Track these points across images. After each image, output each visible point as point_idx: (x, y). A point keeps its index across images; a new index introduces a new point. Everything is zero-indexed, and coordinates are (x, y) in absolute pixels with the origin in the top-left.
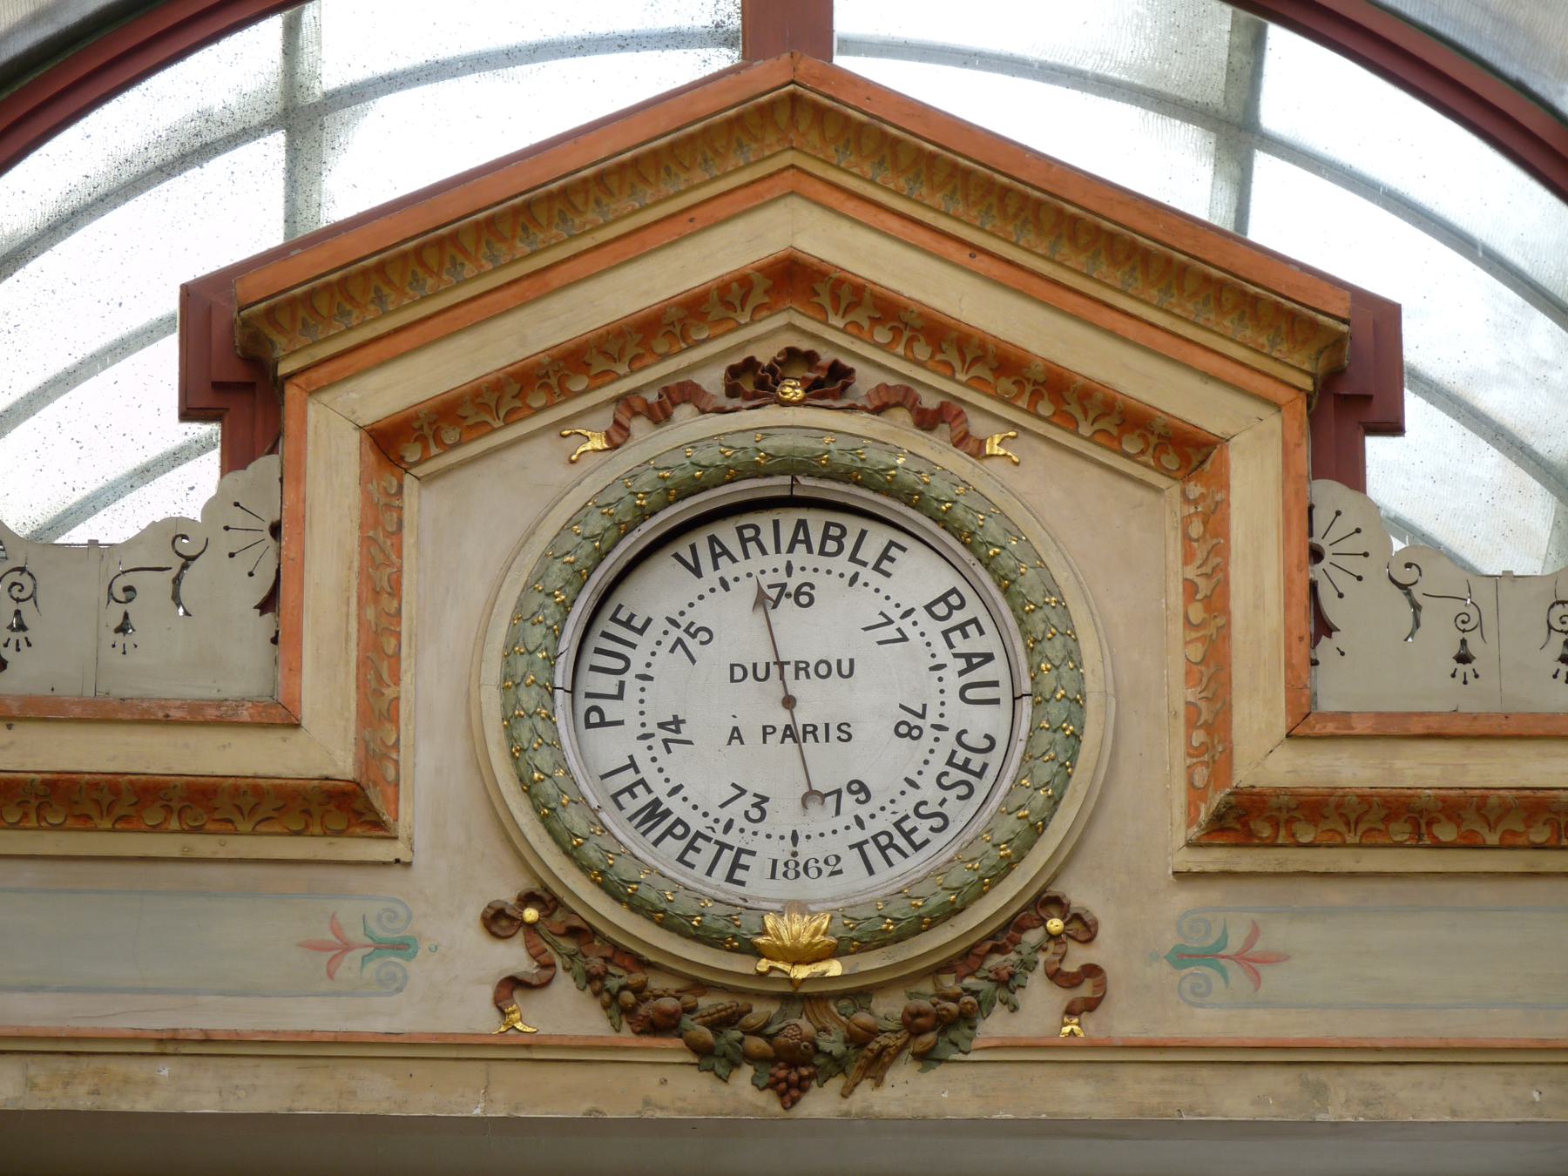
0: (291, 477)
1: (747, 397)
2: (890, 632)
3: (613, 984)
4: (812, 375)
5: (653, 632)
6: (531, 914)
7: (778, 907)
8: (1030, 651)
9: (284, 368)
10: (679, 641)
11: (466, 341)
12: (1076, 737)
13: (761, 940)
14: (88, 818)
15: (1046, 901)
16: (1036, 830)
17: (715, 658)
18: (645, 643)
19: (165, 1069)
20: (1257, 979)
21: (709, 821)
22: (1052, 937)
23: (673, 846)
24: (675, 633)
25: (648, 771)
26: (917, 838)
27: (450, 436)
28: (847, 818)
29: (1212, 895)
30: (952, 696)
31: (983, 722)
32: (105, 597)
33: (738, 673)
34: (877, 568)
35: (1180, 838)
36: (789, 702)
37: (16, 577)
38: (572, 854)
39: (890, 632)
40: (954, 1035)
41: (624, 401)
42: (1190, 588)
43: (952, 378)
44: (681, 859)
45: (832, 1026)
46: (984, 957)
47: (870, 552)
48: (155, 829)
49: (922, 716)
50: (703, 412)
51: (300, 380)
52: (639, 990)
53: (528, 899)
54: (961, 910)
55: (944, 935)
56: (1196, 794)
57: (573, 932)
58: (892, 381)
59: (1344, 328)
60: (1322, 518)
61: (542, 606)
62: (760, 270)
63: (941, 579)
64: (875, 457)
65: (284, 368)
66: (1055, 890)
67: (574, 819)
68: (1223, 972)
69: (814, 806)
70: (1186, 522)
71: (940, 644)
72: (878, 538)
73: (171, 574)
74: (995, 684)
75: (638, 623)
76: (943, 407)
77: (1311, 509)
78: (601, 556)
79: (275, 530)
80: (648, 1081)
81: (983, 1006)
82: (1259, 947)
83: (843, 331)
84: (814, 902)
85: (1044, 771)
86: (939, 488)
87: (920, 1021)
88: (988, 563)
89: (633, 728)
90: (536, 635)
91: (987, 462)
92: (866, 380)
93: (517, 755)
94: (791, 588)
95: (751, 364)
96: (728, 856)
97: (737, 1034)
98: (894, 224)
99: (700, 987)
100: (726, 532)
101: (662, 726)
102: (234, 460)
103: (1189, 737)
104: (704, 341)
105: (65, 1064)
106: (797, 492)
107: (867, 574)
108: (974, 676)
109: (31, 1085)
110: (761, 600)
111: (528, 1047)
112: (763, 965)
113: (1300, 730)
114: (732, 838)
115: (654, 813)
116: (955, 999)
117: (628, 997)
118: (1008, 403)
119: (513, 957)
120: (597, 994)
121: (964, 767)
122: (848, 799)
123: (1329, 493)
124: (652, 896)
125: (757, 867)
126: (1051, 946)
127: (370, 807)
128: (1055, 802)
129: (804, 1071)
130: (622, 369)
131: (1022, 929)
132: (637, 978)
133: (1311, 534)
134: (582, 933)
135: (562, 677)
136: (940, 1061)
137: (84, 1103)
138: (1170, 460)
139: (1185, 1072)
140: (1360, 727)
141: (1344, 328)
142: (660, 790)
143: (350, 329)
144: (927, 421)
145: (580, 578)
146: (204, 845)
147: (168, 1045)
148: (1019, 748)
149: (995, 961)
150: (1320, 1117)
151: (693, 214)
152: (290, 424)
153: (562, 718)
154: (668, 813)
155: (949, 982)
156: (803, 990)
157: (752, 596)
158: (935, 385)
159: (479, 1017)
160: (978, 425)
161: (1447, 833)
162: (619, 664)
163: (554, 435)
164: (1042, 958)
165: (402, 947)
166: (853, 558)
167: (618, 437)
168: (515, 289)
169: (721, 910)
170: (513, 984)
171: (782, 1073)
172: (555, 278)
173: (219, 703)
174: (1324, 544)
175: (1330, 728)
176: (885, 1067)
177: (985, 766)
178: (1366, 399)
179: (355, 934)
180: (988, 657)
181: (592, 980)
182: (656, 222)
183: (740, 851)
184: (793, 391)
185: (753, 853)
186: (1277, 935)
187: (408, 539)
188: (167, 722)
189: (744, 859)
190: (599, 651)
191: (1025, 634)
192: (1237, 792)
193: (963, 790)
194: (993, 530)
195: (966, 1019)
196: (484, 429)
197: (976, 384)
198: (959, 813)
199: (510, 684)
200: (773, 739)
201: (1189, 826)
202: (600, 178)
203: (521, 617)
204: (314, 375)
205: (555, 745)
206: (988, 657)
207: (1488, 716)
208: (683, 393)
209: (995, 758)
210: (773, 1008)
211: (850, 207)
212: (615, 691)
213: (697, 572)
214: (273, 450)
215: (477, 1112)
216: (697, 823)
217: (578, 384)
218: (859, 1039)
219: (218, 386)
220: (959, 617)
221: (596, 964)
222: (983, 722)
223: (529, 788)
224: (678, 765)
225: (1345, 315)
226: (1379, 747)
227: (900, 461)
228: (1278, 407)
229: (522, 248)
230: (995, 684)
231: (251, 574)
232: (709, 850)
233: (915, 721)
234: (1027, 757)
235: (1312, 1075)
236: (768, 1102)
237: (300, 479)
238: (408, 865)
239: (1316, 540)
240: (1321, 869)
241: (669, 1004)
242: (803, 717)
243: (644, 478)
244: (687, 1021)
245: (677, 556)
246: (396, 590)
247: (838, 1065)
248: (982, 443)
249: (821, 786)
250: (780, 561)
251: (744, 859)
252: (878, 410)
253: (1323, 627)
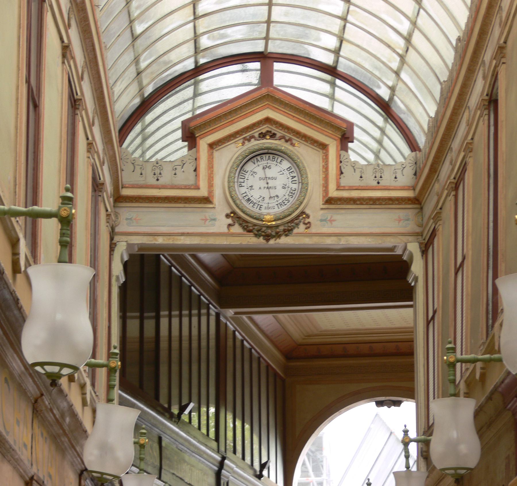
0: (198, 152)
1: (262, 138)
2: (281, 173)
3: (244, 225)
4: (271, 134)
5: (249, 173)
6: (232, 215)
7: (266, 214)
8: (301, 176)
9: (197, 136)
10: (252, 174)
11: (222, 131)
12: (307, 189)
13: (264, 219)
14: (170, 201)
15: (303, 213)
16: (301, 203)
17: (257, 176)
18: (247, 174)
19: (182, 238)
20: (332, 223)
21: (256, 201)
22: (304, 218)
23: (252, 205)
24: (252, 173)
25: (248, 194)
26: (285, 203)
27: (220, 144)
28: (275, 201)
29: (326, 211)
30: (290, 182)
31: (295, 186)
32: (172, 169)
33: (260, 179)
34: (280, 163)
35: (321, 203)
36: (267, 183)
37: (159, 167)
38: (238, 207)
39: (281, 173)
40: (290, 232)
41: (244, 138)
42: (323, 166)
43: (290, 134)
44: (253, 206)
45: (274, 231)
46: (294, 221)
47: (279, 161)
48: (180, 203)
49: (286, 185)
50: (255, 140)
51: (199, 137)
52: (247, 226)
53: (231, 213)
54: (291, 214)
55: (289, 218)
56: (324, 197)
57: (238, 218)
58: (282, 135)
59: (345, 129)
60: (342, 156)
61: (233, 170)
62: (263, 119)
63: (289, 165)
64: (279, 147)
65: (197, 136)
66: (305, 211)
67: (238, 202)
68: (327, 222)
69: (271, 199)
70: (323, 156)
71: (288, 175)
72: (280, 159)
73: (182, 166)
74: (296, 181)
75: (246, 171)
76: (289, 139)
77: (340, 155)
78: (241, 162)
79: (196, 159)
80: (248, 239)
81: (294, 228)
82: (332, 219)
83: (275, 127)
84: (271, 213)
85: (303, 194)
86: (288, 152)
87: (286, 230)
88: (295, 163)
89: (246, 187)
90: (232, 175)
91: (295, 147)
92: (278, 135)
93: (230, 193)
94: (268, 166)
95: (262, 133)
96: (259, 206)
97: (260, 232)
98: (282, 112)
99: (255, 225)
100: (259, 158)
101: (250, 187)
102: (190, 148)
103: (323, 188)
104: (255, 129)
105: (169, 237)
106: (269, 152)
107: (278, 164)
108: (293, 180)
109: (164, 240)
110: (264, 168)
111: (232, 234)
112: (264, 223)
113: (338, 189)
114: (259, 203)
115: (249, 200)
116: (290, 227)
117: (245, 227)
118: (298, 138)
119: (230, 221)
120: (241, 226)
121: (292, 193)
122: (276, 198)
123: (343, 153)
124: (249, 213)
125: (263, 207)
126: (304, 219)
127: (210, 200)
128: (304, 199)
129: (270, 238)
130: (244, 134)
131: (300, 217)
132: (246, 224)
133: (340, 159)
134: (239, 218)
135: (236, 180)
136: (288, 236)
137: (171, 243)
138: (321, 147)
139: (322, 237)
140: (346, 188)
141: (345, 129)
142: (250, 196)
143: (206, 129)
144: (287, 141)
145: (238, 166)
146: (187, 205)
147: (183, 234)
148: (299, 190)
149: (296, 221)
150: (340, 243)
151: (254, 111)
152: (198, 144)
153: (236, 186)
154: (250, 200)
155: (289, 224)
156: (270, 226)
157: (262, 168)
158: (288, 136)
159: (225, 230)
160: (294, 142)
161: (358, 203)
162: (244, 177)
163: (234, 143)
164: (302, 221)
165: (214, 220)
166: (276, 162)
167: (243, 143)
168: (228, 123)
169: (259, 215)
170: (230, 225)
171: (267, 238)
172: (234, 121)
173: (189, 186)
174: (342, 160)
175: (342, 188)
176: (281, 237)
177: (295, 193)
178: (348, 138)
179: (208, 218)
180: (295, 177)
181: (240, 225)
182: (248, 113)
183: (261, 205)
184: (268, 137)
185: (262, 206)
186: (335, 217)
187: (214, 160)
188: (182, 189)
189: (261, 207)
190: (241, 176)
191: (301, 174)
192: (329, 198)
193: (291, 196)
194: (296, 158)
195: (292, 230)
196: (224, 143)
197: (294, 135)
198: (291, 200)
199: (229, 182)
200: (265, 188)
201: (323, 201)
202: (241, 107)
203: (230, 172)
204: (201, 136)
205: (235, 191)
206: (295, 177)
207: (364, 186)
208: (253, 137)
209: (296, 192)
210: (265, 228)
211: (276, 110)
212: (243, 181)
213: (254, 163)
214: (195, 147)
215: (225, 243)
216: (255, 201)
217: (238, 136)
218: (277, 233)
219: (187, 137)
220: (291, 171)
221: (241, 222)
222: (295, 186)
223: (232, 197)
224: (252, 193)
225: (345, 127)
226: (349, 191)
227: (283, 148)
228: (336, 140)
229: (230, 117)
230: (296, 181)
231: (193, 166)
232: (256, 205)
233: (285, 186)
234: (301, 192)
235: (339, 237)
236: (264, 241)
237: (199, 152)
238: (215, 208)
239: (341, 160)
240: (341, 208)
241: (251, 228)
242: (269, 185)
243: (247, 151)
244: (254, 230)
245: (252, 161)
246: (212, 167)
247: (273, 237)
248: (294, 144)
249: (272, 196)
250: (266, 162)
251: (261, 207)
252: (280, 140)
253: (342, 173)
